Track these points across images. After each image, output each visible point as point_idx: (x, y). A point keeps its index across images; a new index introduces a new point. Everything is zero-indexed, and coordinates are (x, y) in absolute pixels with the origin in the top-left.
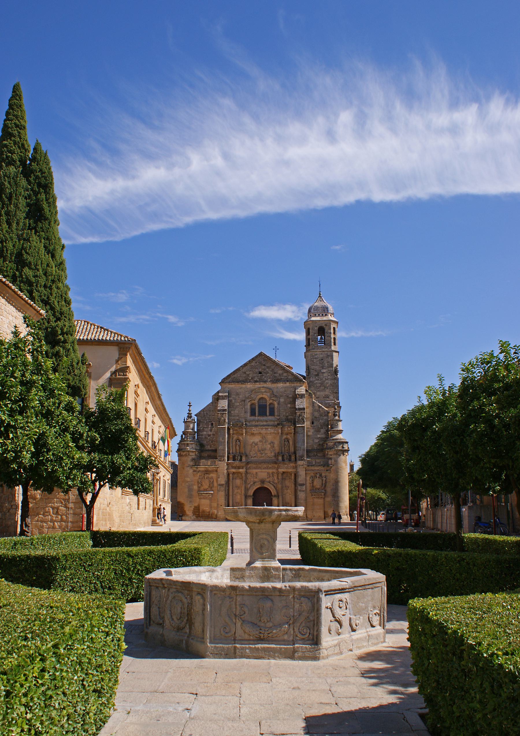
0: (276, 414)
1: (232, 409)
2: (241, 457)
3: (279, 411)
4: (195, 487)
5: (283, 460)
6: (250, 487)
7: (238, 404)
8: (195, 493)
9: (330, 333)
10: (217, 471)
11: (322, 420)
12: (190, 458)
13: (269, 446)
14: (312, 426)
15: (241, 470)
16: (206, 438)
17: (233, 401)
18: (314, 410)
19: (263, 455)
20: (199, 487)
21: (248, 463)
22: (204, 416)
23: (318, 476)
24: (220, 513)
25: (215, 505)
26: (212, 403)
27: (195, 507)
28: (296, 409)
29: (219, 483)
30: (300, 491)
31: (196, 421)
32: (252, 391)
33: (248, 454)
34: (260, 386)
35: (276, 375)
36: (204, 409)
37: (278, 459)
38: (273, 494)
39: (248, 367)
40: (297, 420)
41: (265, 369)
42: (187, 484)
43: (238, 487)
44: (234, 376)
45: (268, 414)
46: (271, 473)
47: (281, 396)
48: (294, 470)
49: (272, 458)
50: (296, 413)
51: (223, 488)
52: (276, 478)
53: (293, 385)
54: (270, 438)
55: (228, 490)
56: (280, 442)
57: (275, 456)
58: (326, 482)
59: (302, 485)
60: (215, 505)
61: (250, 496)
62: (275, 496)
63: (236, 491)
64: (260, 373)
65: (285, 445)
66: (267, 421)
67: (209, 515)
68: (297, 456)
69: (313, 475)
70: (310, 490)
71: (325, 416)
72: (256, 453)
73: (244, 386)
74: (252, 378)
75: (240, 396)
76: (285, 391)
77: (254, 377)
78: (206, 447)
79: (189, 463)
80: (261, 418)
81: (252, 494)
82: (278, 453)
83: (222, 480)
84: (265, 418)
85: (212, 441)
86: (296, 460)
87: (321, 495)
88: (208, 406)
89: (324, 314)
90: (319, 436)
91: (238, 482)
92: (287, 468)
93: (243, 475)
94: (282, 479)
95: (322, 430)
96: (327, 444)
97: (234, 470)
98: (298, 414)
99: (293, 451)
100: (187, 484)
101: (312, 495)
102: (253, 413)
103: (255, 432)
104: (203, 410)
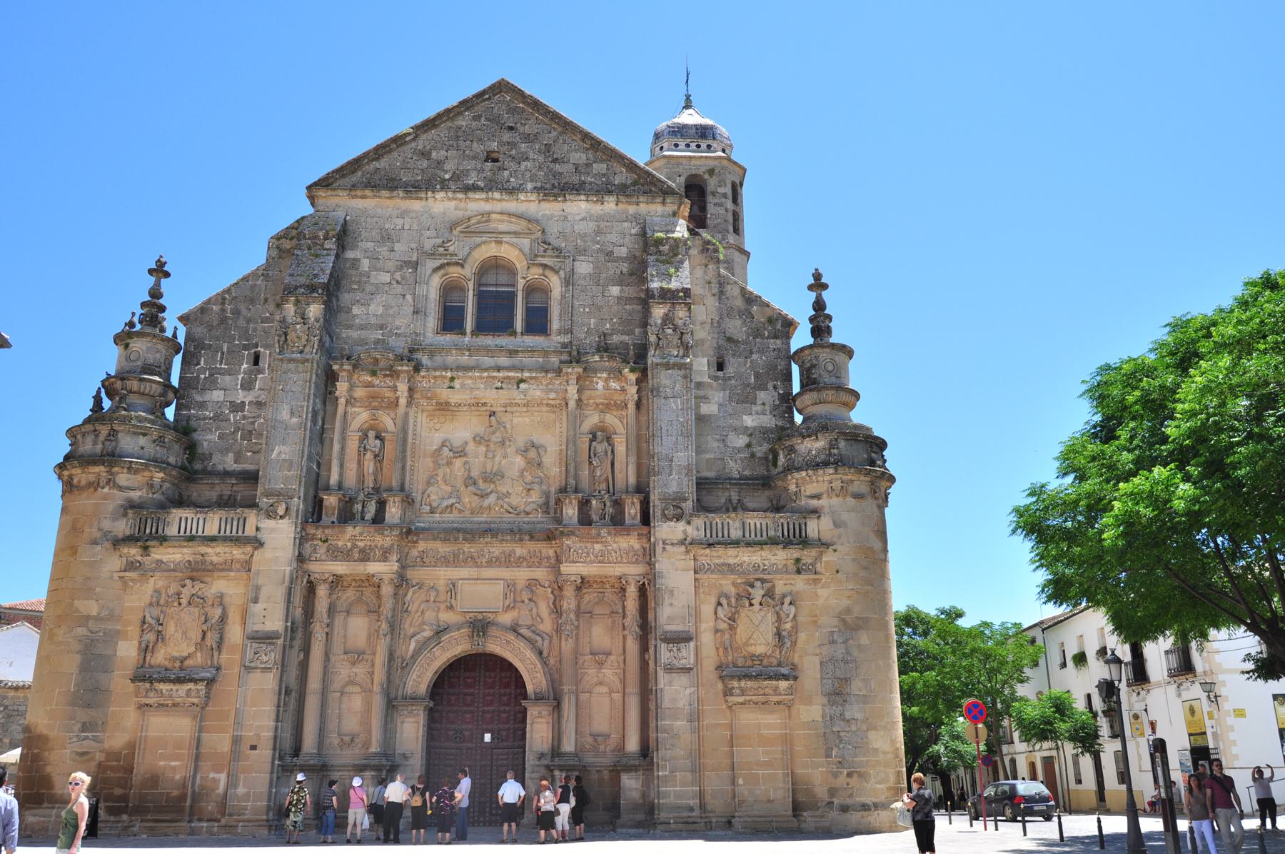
0: (555, 325)
1: (359, 295)
2: (382, 505)
3: (569, 310)
4: (127, 651)
5: (585, 520)
6: (417, 653)
7: (386, 278)
8: (119, 682)
9: (725, 196)
10: (247, 566)
11: (761, 351)
12: (119, 497)
13: (519, 461)
14: (716, 378)
15: (374, 567)
16: (218, 417)
17: (365, 264)
18: (726, 312)
19: (486, 503)
20: (145, 650)
21: (409, 533)
22: (223, 320)
23: (758, 593)
24: (241, 790)
25: (219, 742)
26: (268, 265)
27: (111, 755)
28: (649, 294)
29: (255, 626)
30: (670, 669)
31: (181, 340)
32: (452, 227)
33: (418, 497)
34: (487, 207)
35: (558, 167)
36: (228, 291)
37: (559, 521)
38: (530, 688)
39: (441, 132)
40: (653, 338)
41: (512, 145)
42: (81, 631)
43: (356, 656)
44: (376, 164)
45: (519, 324)
46: (521, 584)
47: (582, 252)
48: (634, 571)
49: (532, 518)
50: (645, 324)
51: (270, 656)
52: (544, 609)
53: (632, 209)
54: (523, 425)
55: (304, 666)
56: (572, 441)
57: (545, 507)
58: (795, 629)
59: (681, 639)
60: (219, 742)
61: (414, 698)
62: (539, 698)
63: (343, 671)
64: (491, 158)
65: (592, 454)
66: (512, 353)
67: (183, 797)
68: (654, 498)
69: (732, 591)
70: (719, 667)
71: (776, 337)
72: (455, 492)
73: (416, 205)
74: (456, 177)
75: (397, 247)
76: (598, 232)
77: (466, 173)
78: (216, 459)
79: (106, 525)
80: (488, 340)
81: (423, 689)
82: (563, 490)
83: (272, 617)
84: (504, 341)
85: (248, 435)
86: (646, 519)
87: (776, 689)
88: (245, 279)
89: (704, 146)
90: (749, 421)
91: (357, 628)
92: (602, 559)
93: (387, 590)
94: (579, 613)
95: (762, 395)
96: (792, 450)
97: (340, 568)
98: (658, 312)
99: (632, 480)
100: (81, 631)
101: (728, 692)
102: (451, 320)
103: (455, 397)
104: (221, 298)
